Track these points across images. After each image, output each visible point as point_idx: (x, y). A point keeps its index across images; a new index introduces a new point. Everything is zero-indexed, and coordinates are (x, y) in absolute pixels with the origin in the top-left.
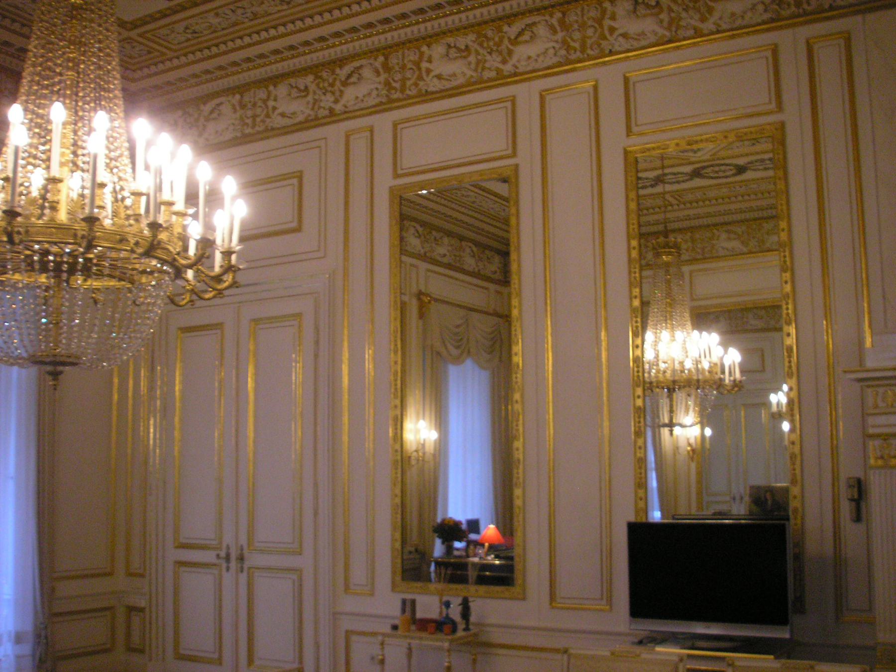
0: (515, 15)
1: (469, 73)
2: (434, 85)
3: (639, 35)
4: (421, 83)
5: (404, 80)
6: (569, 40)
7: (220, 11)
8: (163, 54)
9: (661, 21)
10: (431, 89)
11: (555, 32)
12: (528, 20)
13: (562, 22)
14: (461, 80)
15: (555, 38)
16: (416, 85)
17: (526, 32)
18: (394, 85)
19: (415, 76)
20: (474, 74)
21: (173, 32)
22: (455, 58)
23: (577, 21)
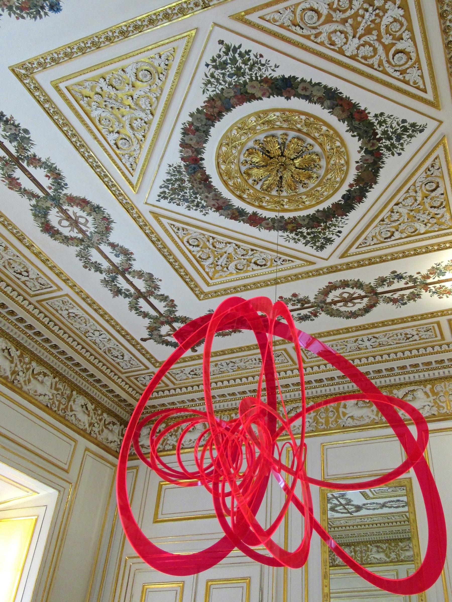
0: (401, 385)
1: (373, 417)
2: (350, 422)
3: (359, 418)
4: (340, 421)
5: (327, 418)
6: (438, 402)
7: (219, 363)
8: (167, 385)
9: (373, 411)
10: (347, 425)
11: (428, 396)
12: (412, 388)
13: (432, 390)
14: (367, 421)
15: (429, 400)
16: (337, 422)
17: (409, 395)
18: (320, 420)
19: (335, 416)
20: (376, 418)
21: (182, 372)
22: (362, 407)
23: (442, 391)
